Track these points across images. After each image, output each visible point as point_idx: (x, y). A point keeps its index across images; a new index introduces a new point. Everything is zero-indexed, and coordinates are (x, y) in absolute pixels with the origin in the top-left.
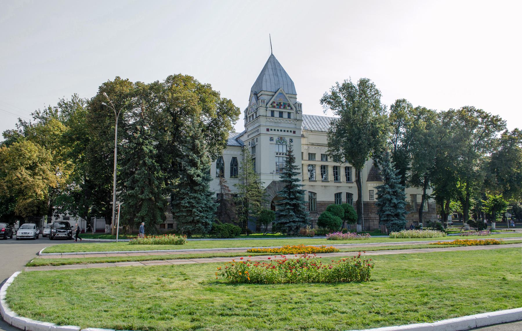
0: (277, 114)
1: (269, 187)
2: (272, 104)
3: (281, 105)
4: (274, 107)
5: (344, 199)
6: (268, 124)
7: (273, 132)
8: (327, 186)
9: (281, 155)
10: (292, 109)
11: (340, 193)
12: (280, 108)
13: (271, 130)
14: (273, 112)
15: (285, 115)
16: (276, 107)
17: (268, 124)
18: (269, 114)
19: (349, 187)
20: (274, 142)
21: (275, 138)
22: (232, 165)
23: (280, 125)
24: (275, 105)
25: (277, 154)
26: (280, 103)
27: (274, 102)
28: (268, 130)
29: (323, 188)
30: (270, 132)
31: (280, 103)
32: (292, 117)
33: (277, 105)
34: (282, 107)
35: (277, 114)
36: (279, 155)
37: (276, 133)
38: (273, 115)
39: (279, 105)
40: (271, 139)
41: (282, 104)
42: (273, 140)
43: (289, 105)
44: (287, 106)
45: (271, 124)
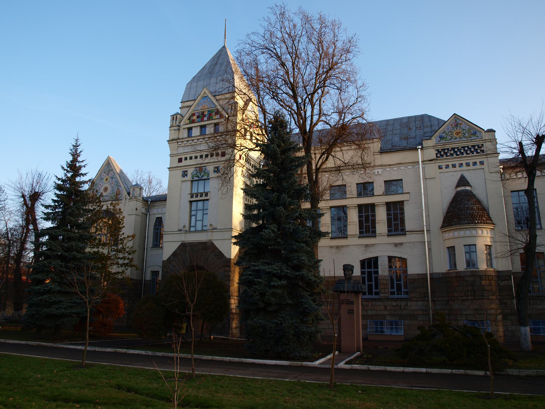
0: (196, 132)
1: (174, 254)
2: (189, 119)
3: (204, 116)
4: (193, 122)
5: (383, 270)
6: (181, 150)
7: (189, 162)
8: (342, 247)
9: (199, 198)
10: (221, 116)
11: (376, 260)
12: (202, 120)
13: (186, 159)
14: (190, 129)
15: (210, 130)
16: (197, 120)
17: (181, 150)
18: (184, 134)
19: (396, 245)
20: (189, 177)
21: (190, 171)
22: (155, 225)
23: (199, 148)
24: (195, 118)
25: (192, 197)
26: (203, 113)
27: (193, 115)
28: (180, 160)
29: (334, 250)
30: (184, 163)
31: (203, 113)
32: (221, 129)
33: (198, 117)
34: (205, 119)
35: (196, 132)
36: (194, 199)
37: (193, 162)
38: (189, 135)
39: (201, 116)
40: (185, 174)
41: (206, 113)
42: (186, 175)
43: (217, 112)
44: (213, 114)
45: (187, 150)
